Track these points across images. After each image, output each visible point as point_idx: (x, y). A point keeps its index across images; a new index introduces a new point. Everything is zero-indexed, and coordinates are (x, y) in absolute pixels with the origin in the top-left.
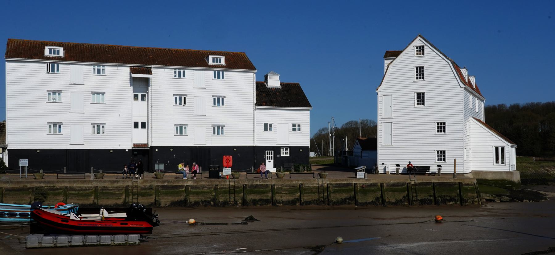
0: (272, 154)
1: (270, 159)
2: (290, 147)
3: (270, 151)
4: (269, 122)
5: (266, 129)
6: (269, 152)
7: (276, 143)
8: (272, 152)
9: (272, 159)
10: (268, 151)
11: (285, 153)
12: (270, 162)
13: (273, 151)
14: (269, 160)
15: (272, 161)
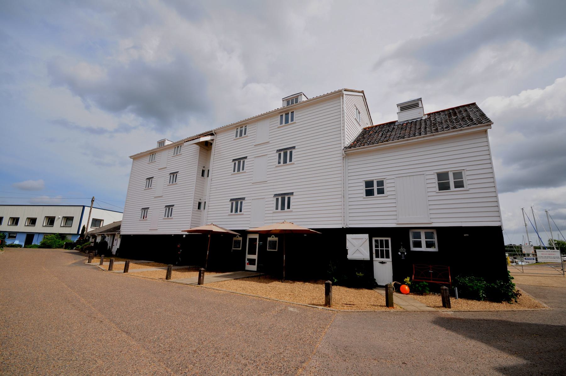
0: (387, 246)
1: (382, 257)
2: (439, 229)
3: (384, 239)
4: (375, 178)
5: (369, 193)
6: (382, 241)
7: (395, 221)
8: (387, 242)
9: (388, 257)
10: (379, 239)
11: (424, 244)
12: (382, 263)
13: (389, 239)
14: (380, 259)
15: (389, 262)
